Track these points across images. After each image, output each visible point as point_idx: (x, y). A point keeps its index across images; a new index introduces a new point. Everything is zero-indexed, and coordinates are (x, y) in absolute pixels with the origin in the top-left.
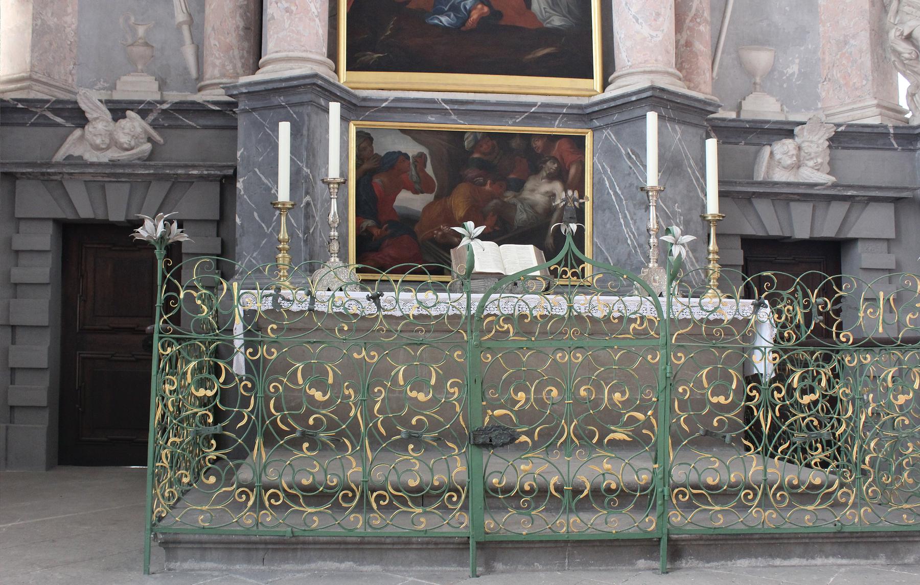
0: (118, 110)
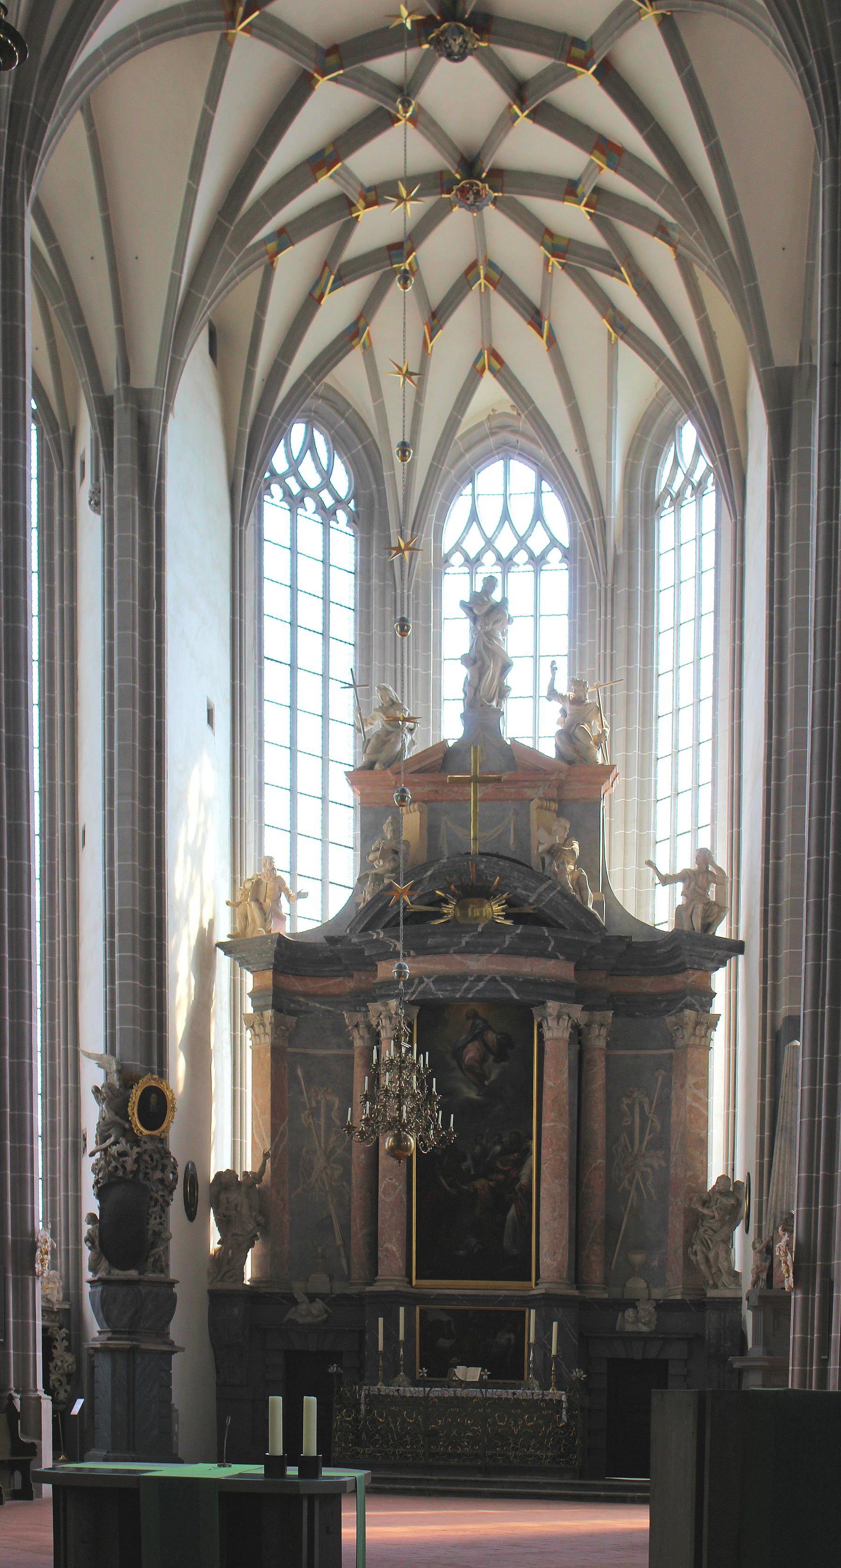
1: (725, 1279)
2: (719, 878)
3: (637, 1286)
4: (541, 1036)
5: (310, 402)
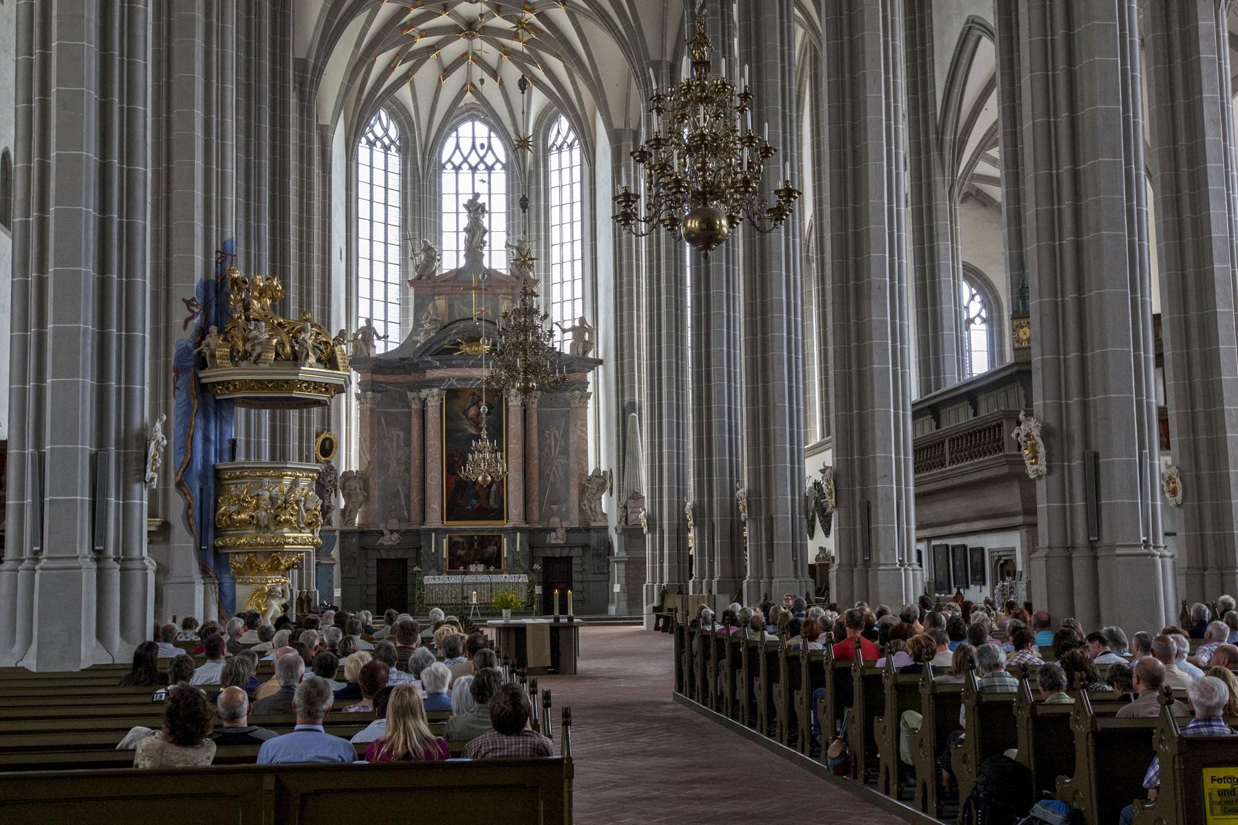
0: (392, 532)
1: (599, 517)
2: (590, 331)
3: (555, 521)
4: (507, 405)
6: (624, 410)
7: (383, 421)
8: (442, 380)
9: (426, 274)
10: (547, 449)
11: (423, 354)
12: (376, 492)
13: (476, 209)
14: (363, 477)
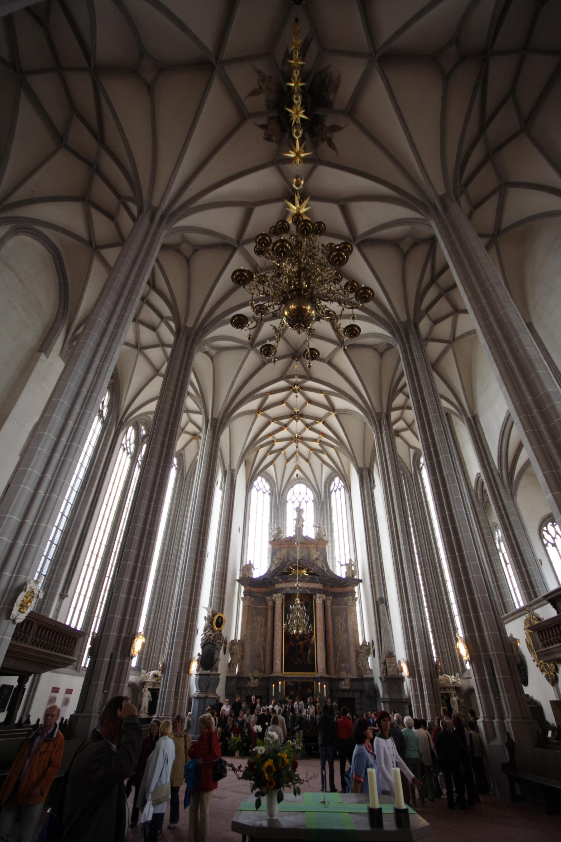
1: (368, 671)
3: (343, 674)
5: (263, 474)
6: (377, 602)
7: (254, 612)
8: (282, 589)
9: (277, 539)
10: (337, 629)
11: (274, 575)
12: (248, 653)
13: (299, 511)
14: (242, 643)
